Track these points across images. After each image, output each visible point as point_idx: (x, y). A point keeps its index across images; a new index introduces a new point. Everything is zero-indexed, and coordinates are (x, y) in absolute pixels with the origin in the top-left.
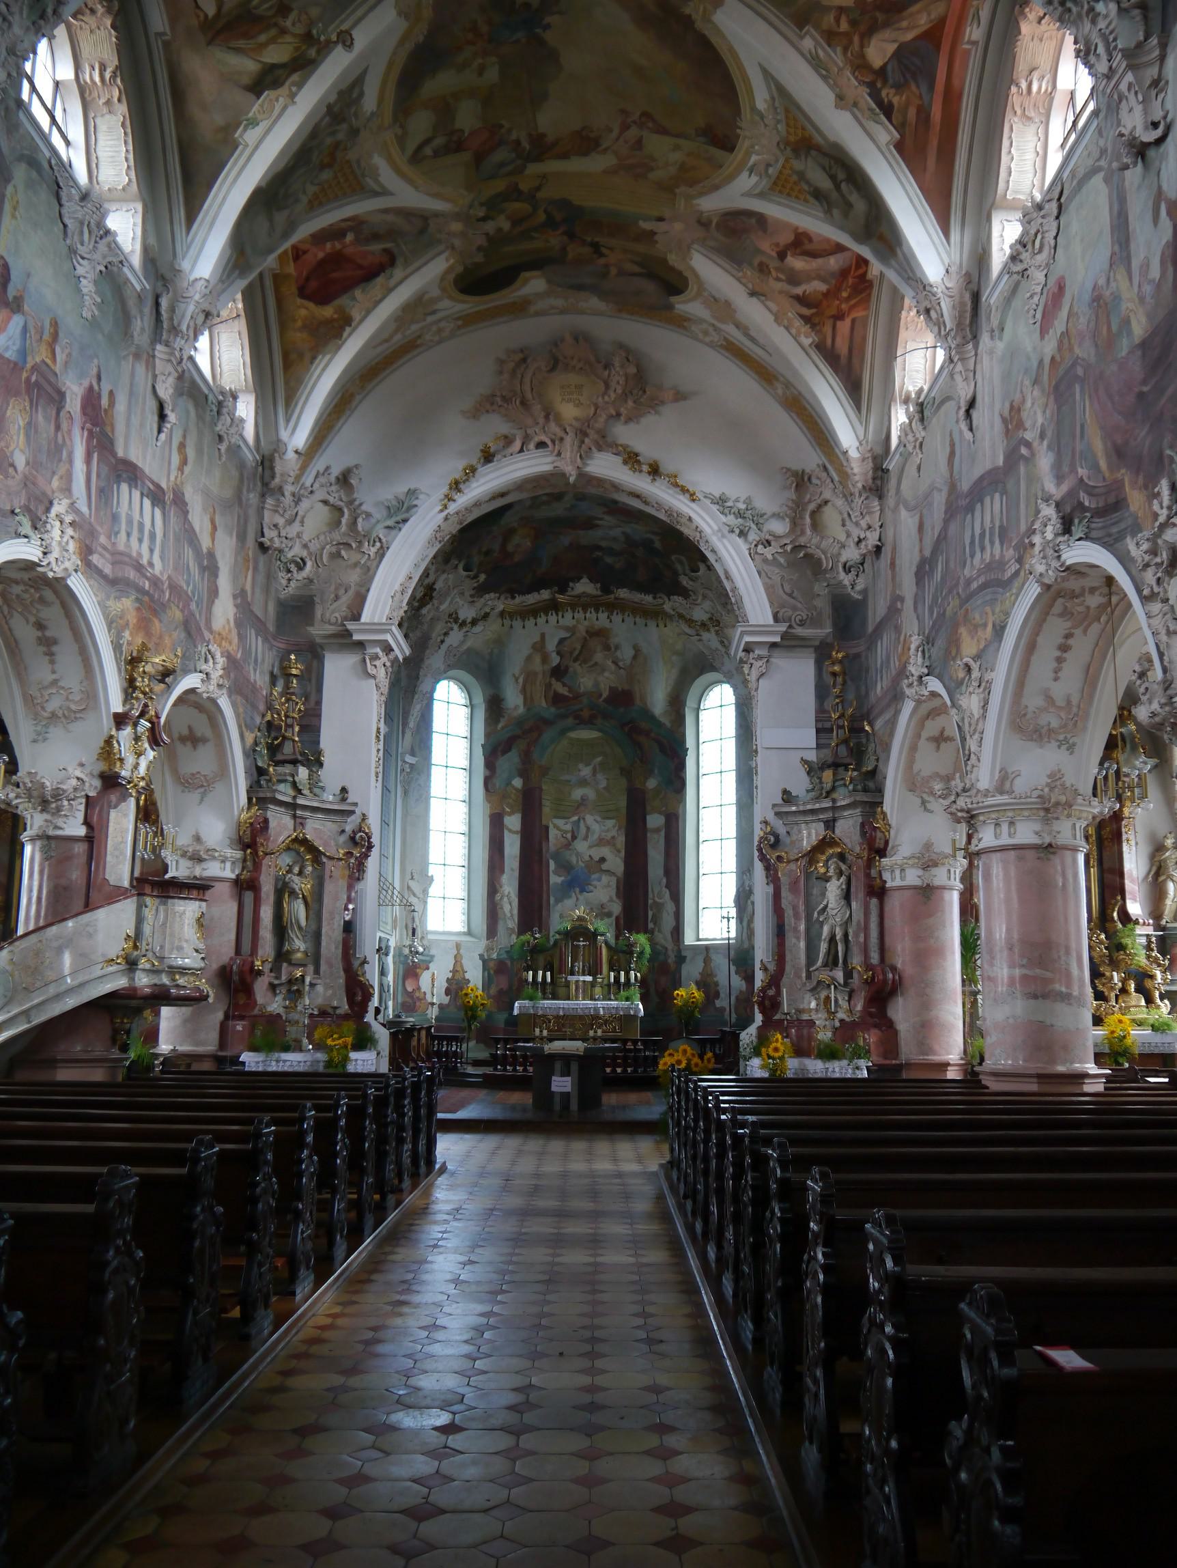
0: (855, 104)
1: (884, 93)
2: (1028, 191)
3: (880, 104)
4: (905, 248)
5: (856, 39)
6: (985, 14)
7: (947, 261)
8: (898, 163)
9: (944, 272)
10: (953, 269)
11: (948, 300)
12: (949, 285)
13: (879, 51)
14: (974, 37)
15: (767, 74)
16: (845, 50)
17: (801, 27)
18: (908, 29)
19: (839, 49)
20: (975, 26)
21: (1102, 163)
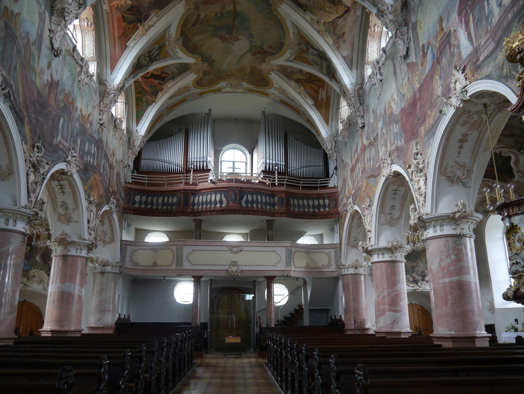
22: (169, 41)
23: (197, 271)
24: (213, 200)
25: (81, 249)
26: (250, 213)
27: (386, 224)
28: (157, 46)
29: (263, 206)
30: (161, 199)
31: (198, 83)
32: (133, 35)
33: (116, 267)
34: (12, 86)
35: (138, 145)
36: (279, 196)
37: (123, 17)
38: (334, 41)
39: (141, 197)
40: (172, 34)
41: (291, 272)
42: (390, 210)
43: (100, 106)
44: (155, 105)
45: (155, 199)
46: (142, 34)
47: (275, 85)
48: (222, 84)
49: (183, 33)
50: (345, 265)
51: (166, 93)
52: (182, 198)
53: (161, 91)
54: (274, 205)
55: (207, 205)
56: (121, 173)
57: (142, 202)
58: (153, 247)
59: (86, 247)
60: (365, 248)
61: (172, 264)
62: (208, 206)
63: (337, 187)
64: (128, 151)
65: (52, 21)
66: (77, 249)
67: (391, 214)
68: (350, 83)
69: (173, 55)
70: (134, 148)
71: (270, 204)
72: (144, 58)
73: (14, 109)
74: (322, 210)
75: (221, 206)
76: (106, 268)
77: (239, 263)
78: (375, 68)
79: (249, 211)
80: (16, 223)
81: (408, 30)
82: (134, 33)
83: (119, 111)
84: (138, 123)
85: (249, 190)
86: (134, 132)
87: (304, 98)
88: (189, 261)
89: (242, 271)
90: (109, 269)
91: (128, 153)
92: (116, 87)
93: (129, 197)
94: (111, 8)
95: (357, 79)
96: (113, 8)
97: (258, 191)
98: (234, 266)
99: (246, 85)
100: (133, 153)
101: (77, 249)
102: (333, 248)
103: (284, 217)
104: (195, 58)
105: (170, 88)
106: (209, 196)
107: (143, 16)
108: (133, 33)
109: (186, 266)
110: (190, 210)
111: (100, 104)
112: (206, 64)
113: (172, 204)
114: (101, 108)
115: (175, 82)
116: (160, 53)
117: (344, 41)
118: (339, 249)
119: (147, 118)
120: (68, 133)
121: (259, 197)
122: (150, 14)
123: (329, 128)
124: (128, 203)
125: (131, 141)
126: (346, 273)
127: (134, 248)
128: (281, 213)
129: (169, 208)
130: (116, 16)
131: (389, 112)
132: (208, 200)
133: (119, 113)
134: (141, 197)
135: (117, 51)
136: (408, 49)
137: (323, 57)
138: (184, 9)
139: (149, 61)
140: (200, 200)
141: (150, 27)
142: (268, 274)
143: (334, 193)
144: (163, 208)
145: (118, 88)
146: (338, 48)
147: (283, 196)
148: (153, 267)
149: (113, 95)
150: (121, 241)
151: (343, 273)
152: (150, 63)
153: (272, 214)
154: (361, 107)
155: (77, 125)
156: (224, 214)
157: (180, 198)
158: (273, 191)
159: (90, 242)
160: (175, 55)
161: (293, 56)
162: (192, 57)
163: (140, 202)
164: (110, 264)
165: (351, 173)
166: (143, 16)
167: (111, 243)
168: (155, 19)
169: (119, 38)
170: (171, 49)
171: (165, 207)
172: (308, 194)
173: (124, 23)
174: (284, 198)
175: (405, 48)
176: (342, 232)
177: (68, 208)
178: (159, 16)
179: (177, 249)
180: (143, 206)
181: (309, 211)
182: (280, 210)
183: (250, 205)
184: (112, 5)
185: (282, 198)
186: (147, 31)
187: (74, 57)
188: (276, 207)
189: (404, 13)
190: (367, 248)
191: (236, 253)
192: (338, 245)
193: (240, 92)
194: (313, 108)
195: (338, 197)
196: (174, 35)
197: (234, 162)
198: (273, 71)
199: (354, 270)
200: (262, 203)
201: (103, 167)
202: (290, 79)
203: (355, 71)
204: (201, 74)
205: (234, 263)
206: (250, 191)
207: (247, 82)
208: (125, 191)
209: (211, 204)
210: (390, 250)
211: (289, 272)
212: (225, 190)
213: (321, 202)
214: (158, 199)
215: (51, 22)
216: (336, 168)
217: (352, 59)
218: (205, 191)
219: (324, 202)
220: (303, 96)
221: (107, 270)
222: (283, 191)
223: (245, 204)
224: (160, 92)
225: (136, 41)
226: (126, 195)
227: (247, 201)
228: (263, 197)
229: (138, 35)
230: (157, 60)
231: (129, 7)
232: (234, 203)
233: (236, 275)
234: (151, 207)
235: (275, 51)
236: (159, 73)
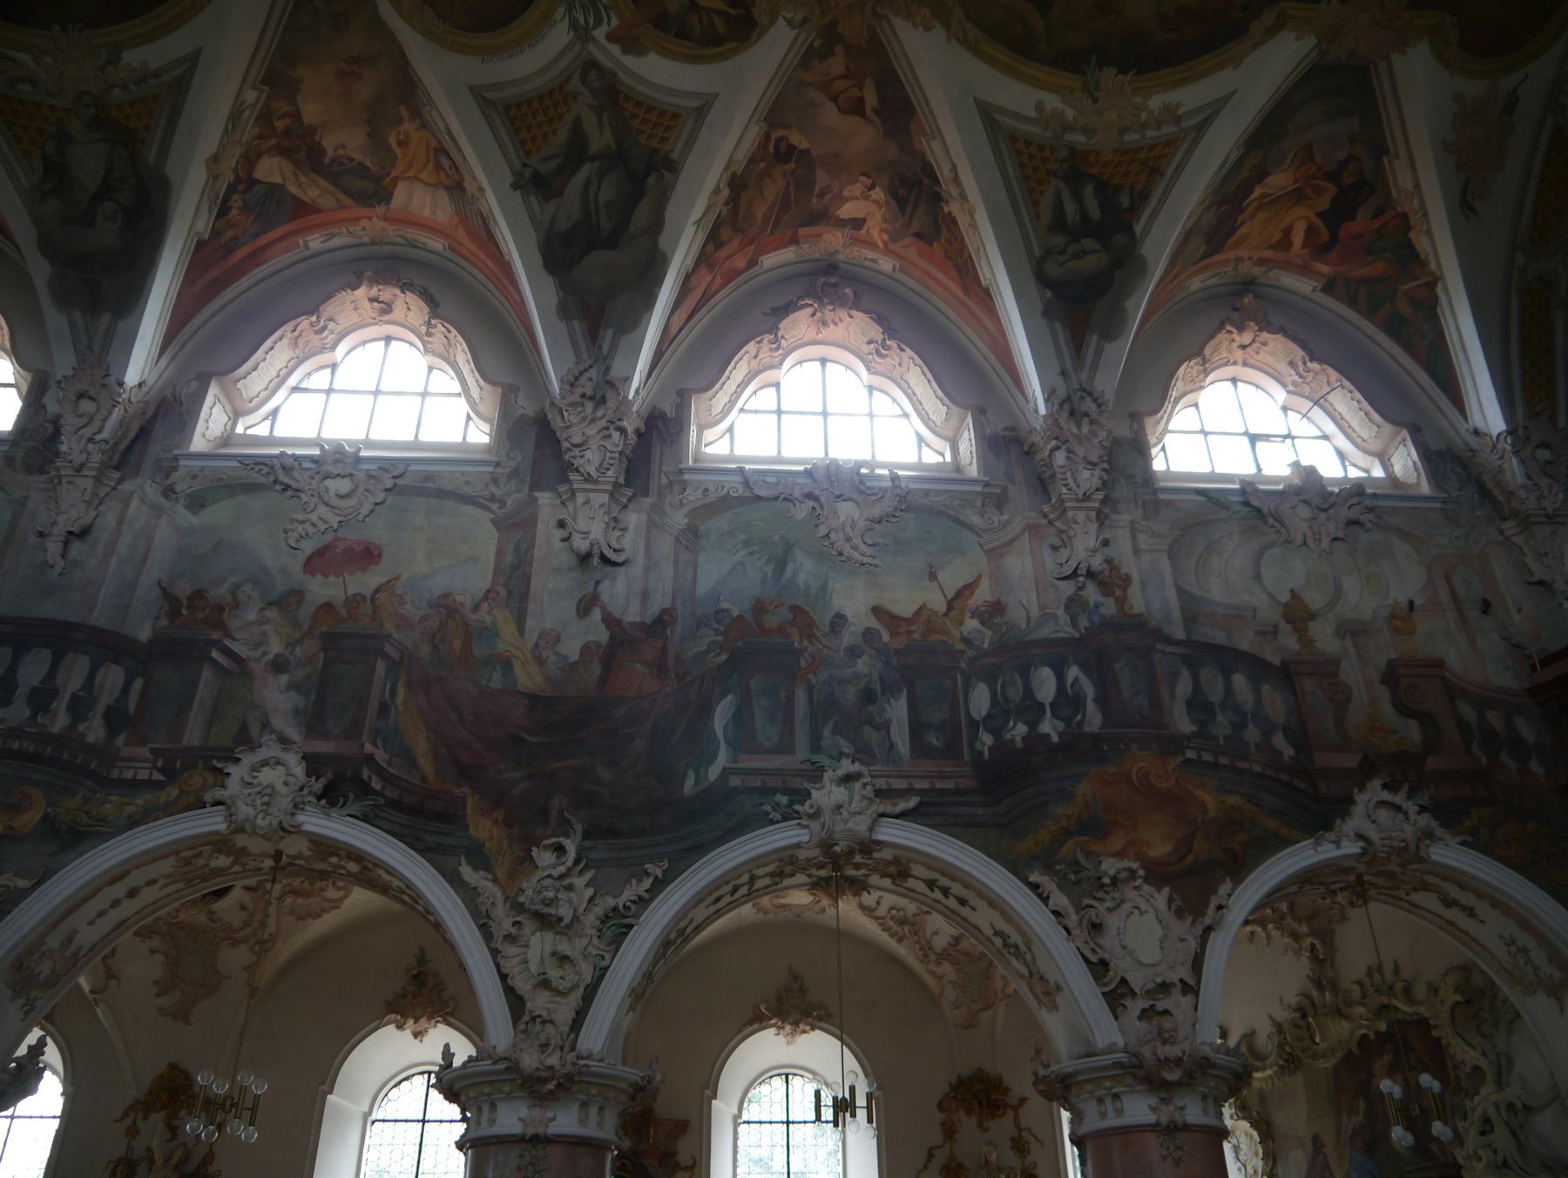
0: (216, 177)
1: (236, 197)
2: (251, 395)
3: (226, 199)
4: (122, 325)
5: (273, 141)
6: (336, 242)
7: (145, 376)
8: (187, 255)
9: (137, 383)
10: (145, 389)
11: (122, 411)
12: (133, 400)
13: (270, 169)
14: (311, 244)
15: (193, 59)
16: (260, 137)
17: (263, 82)
18: (300, 185)
19: (257, 130)
20: (322, 239)
21: (494, 507)
22: (1067, 127)
25: (1116, 1097)
32: (965, 247)
34: (370, 758)
37: (918, 235)
40: (1039, 107)
49: (1070, 61)
51: (1425, 215)
53: (1409, 228)
66: (1100, 1100)
69: (1168, 129)
73: (396, 805)
82: (963, 239)
83: (1357, 429)
84: (1458, 402)
94: (888, 252)
96: (891, 246)
105: (1417, 186)
107: (926, 181)
108: (963, 247)
120: (789, 719)
122: (923, 155)
125: (1490, 485)
130: (912, 253)
133: (1365, 435)
138: (928, 29)
141: (957, 181)
159: (1121, 1057)
160: (1178, 120)
162: (1256, 46)
166: (926, 181)
168: (936, 145)
170: (1124, 130)
173: (935, 244)
178: (931, 128)
184: (881, 245)
186: (963, 197)
187: (759, 498)
196: (1052, 101)
224: (1412, 235)
231: (893, 203)
236: (1331, 190)
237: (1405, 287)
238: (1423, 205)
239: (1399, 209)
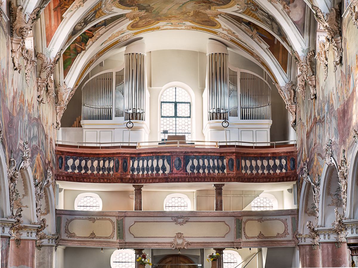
23: (140, 244)
24: (155, 165)
25: (32, 233)
26: (196, 179)
27: (333, 205)
28: (93, 12)
29: (211, 171)
30: (95, 163)
31: (133, 26)
33: (52, 240)
35: (66, 100)
36: (229, 157)
38: (284, 5)
39: (74, 161)
41: (242, 244)
42: (337, 191)
43: (38, 82)
44: (84, 53)
45: (89, 163)
46: (79, 5)
47: (223, 26)
48: (161, 24)
50: (302, 235)
51: (97, 40)
52: (120, 163)
53: (91, 38)
54: (223, 168)
55: (148, 171)
56: (52, 138)
57: (75, 167)
58: (89, 217)
59: (36, 230)
60: (312, 228)
61: (112, 236)
62: (150, 172)
63: (296, 144)
64: (56, 108)
65: (13, 41)
66: (28, 233)
67: (338, 195)
68: (302, 49)
69: (108, 12)
70: (62, 103)
71: (218, 168)
72: (79, 25)
74: (278, 171)
75: (164, 172)
76: (42, 241)
77: (184, 235)
78: (322, 49)
79: (195, 178)
80: (4, 230)
81: (342, 40)
84: (65, 74)
85: (195, 154)
86: (61, 84)
87: (258, 42)
88: (130, 233)
89: (188, 244)
90: (45, 242)
91: (56, 110)
92: (52, 60)
93: (60, 161)
95: (309, 45)
97: (205, 154)
98: (180, 238)
99: (188, 23)
100: (61, 109)
101: (28, 233)
102: (290, 215)
103: (234, 182)
104: (132, 9)
105: (102, 35)
106: (150, 161)
109: (129, 239)
110: (129, 176)
111: (38, 80)
112: (143, 12)
113: (109, 169)
114: (39, 84)
115: (107, 29)
116: (95, 15)
117: (295, 6)
118: (296, 216)
119: (76, 68)
121: (206, 161)
123: (287, 76)
124: (60, 168)
126: (303, 243)
127: (69, 217)
128: (231, 178)
129: (106, 173)
131: (332, 103)
132: (150, 165)
134: (74, 161)
135: (53, 22)
136: (341, 58)
137: (272, 19)
139: (84, 25)
140: (141, 166)
142: (217, 246)
143: (292, 152)
144: (98, 173)
145: (55, 61)
146: (288, 13)
147: (233, 157)
148: (90, 238)
149: (50, 68)
150: (56, 209)
151: (300, 243)
152: (85, 25)
153: (221, 179)
154: (313, 76)
155: (26, 118)
156: (168, 182)
157: (118, 162)
158: (221, 153)
161: (241, 10)
163: (73, 167)
164: (47, 237)
165: (307, 138)
167: (46, 214)
169: (55, 9)
171: (101, 172)
172: (262, 154)
174: (235, 160)
175: (339, 56)
176: (299, 198)
177: (18, 194)
179: (117, 220)
180: (77, 171)
181: (263, 173)
182: (229, 174)
183: (195, 171)
185: (232, 160)
188: (225, 171)
189: (339, 22)
190: (313, 229)
191: (181, 224)
192: (296, 212)
193: (181, 29)
194: (268, 53)
195: (297, 156)
197: (176, 103)
198: (220, 15)
199: (312, 240)
200: (209, 167)
201: (42, 143)
202: (241, 23)
203: (306, 37)
204: (137, 19)
205: (179, 236)
206: (195, 156)
207: (190, 22)
208: (56, 155)
209: (152, 170)
210: (336, 232)
211: (239, 244)
212: (169, 154)
213: (277, 162)
214: (92, 163)
215: (12, 42)
216: (295, 122)
217: (304, 24)
218: (145, 155)
219: (280, 162)
220: (256, 39)
221: (43, 244)
222: (233, 153)
223: (191, 170)
225: (73, 12)
226: (58, 160)
227: (193, 167)
228: (211, 160)
229: (74, 7)
230: (91, 22)
232: (178, 170)
233: (182, 248)
234: (86, 172)
235: (221, 3)
237: (77, 44)
238: (98, 38)
239: (94, 34)
